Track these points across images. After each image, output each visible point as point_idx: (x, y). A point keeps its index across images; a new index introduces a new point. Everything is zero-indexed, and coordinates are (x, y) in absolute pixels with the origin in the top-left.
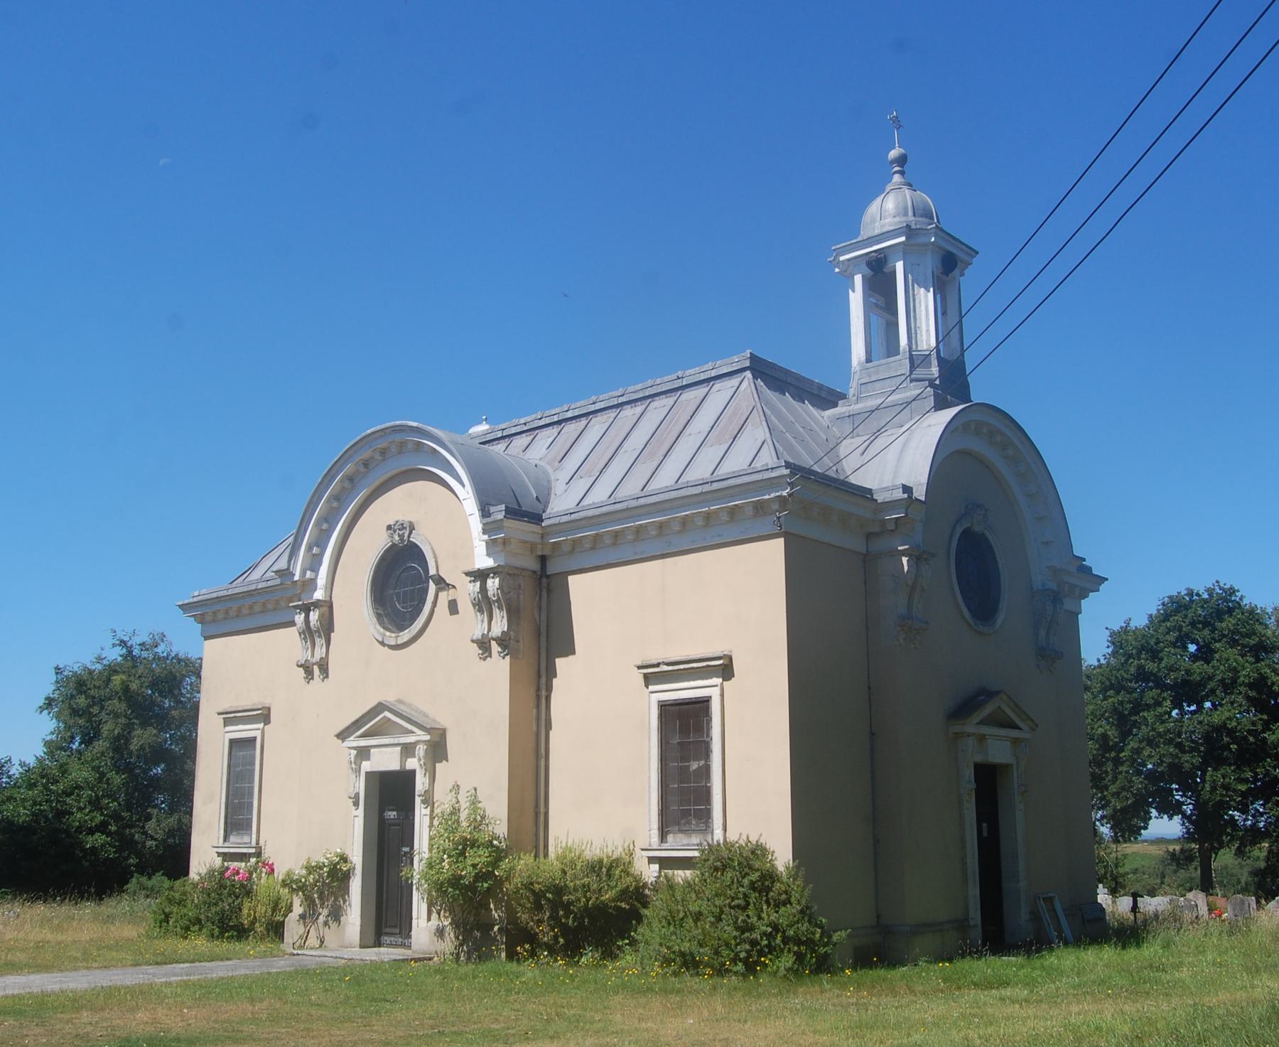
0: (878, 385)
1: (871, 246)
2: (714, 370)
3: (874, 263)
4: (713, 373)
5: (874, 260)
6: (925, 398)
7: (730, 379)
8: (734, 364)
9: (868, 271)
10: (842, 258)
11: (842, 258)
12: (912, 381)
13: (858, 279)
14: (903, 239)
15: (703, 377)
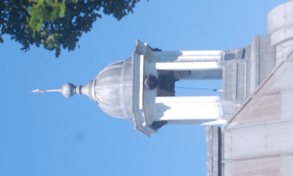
0: (240, 86)
1: (139, 82)
2: (214, 159)
3: (152, 82)
4: (216, 159)
5: (151, 81)
6: (259, 42)
7: (224, 145)
8: (214, 140)
9: (155, 91)
10: (141, 107)
11: (141, 107)
12: (243, 57)
13: (159, 100)
14: (142, 57)
15: (216, 169)
